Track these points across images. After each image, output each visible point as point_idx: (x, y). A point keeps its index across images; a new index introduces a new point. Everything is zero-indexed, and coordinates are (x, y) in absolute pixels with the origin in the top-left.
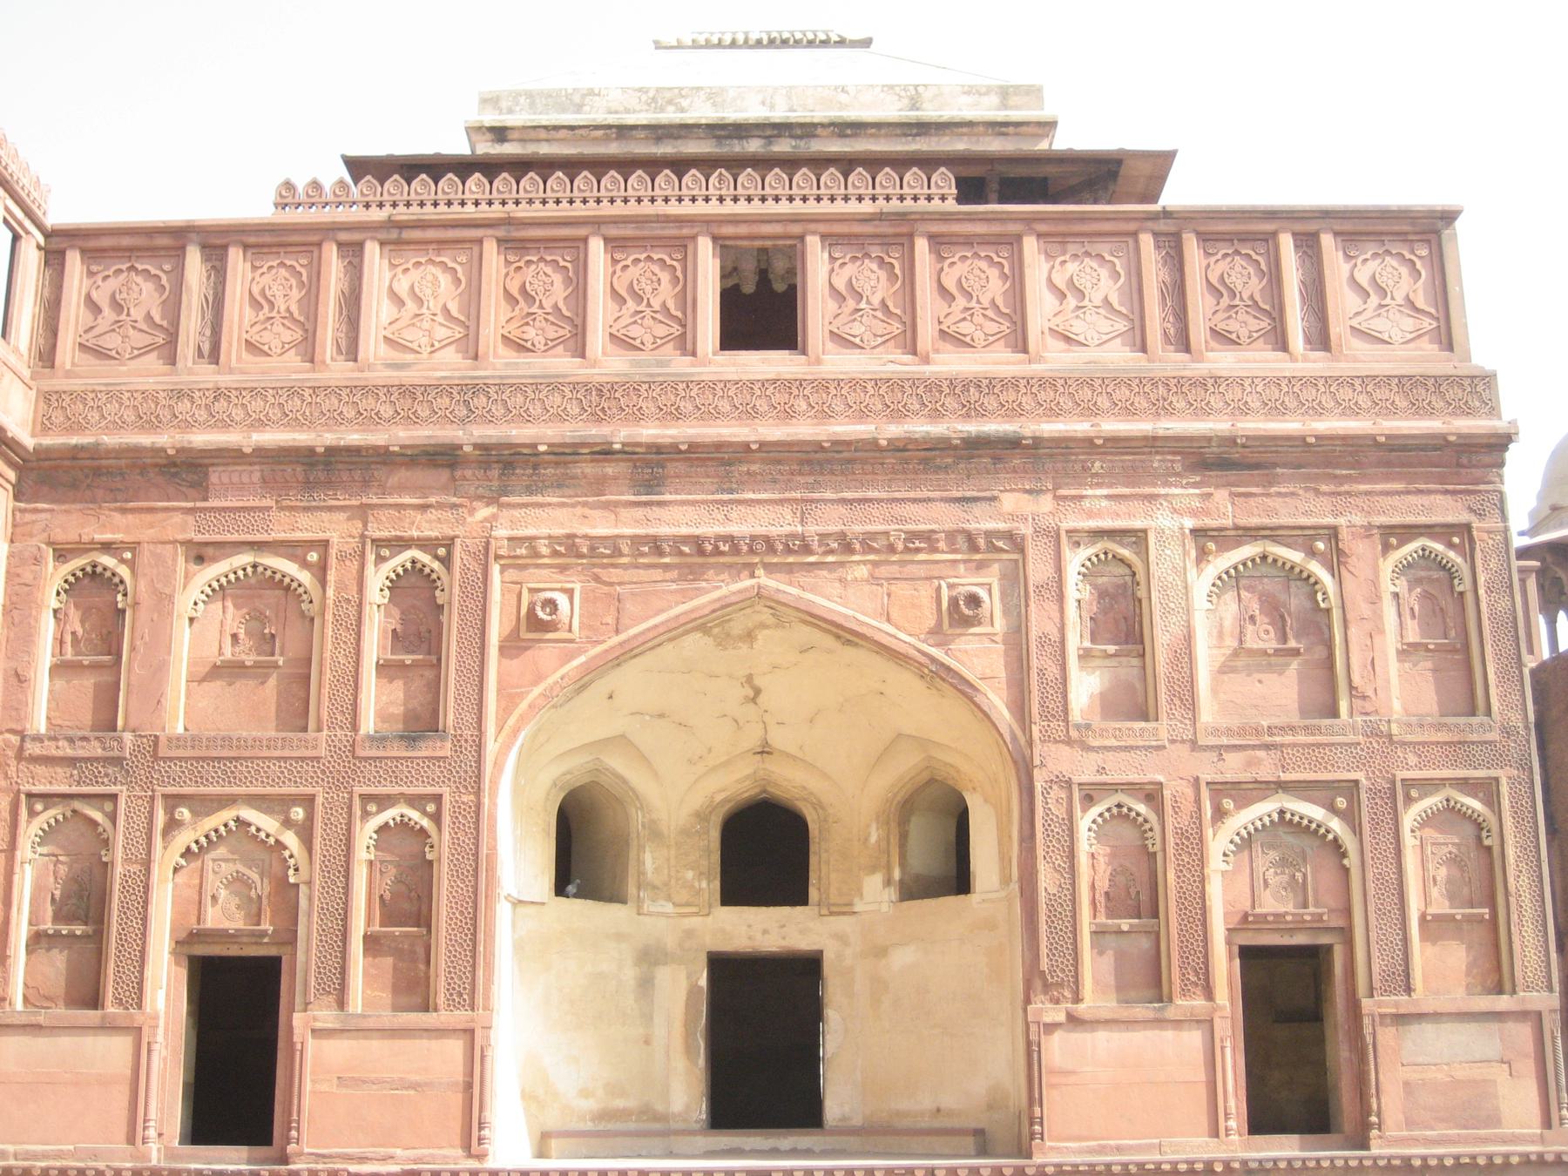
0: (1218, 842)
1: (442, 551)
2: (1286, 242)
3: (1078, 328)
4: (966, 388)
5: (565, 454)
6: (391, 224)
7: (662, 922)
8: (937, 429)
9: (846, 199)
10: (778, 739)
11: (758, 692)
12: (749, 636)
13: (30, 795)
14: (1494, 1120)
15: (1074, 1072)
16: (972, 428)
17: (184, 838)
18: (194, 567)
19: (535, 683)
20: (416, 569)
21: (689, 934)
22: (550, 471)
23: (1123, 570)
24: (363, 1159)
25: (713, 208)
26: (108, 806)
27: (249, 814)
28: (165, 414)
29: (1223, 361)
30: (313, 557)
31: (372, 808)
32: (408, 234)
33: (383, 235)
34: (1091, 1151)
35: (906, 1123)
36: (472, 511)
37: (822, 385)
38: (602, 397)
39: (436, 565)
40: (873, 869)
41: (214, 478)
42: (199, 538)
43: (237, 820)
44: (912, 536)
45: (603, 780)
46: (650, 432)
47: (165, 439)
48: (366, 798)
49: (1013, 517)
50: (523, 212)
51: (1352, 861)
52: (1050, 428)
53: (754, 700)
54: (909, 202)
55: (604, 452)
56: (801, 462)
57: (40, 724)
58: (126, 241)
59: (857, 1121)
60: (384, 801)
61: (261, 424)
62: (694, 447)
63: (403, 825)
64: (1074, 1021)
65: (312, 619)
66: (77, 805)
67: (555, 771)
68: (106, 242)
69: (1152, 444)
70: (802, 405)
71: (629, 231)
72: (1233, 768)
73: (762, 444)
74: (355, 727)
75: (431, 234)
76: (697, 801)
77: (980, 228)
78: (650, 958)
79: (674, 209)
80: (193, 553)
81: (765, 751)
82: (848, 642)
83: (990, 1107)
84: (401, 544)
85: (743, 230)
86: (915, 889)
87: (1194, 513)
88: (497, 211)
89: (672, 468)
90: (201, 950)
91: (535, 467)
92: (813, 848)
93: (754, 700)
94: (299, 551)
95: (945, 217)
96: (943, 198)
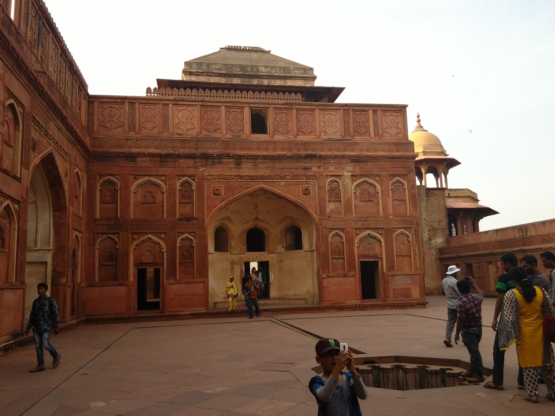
0: (357, 240)
1: (193, 178)
2: (371, 112)
3: (327, 130)
4: (305, 144)
5: (220, 157)
6: (175, 100)
7: (235, 256)
8: (300, 153)
9: (278, 99)
10: (260, 217)
11: (257, 207)
12: (258, 196)
13: (97, 233)
14: (411, 296)
15: (327, 288)
16: (307, 153)
17: (136, 242)
18: (134, 180)
19: (215, 207)
20: (187, 182)
21: (241, 258)
22: (216, 160)
23: (337, 183)
24: (181, 311)
25: (248, 100)
26: (117, 236)
27: (150, 236)
28: (125, 144)
29: (358, 138)
30: (163, 178)
31: (180, 234)
32: (180, 103)
33: (173, 102)
34: (332, 303)
35: (289, 297)
36: (199, 169)
37: (275, 142)
38: (227, 143)
39: (192, 181)
40: (279, 244)
41: (138, 160)
42: (135, 174)
43: (148, 238)
44: (294, 176)
45: (223, 226)
46: (239, 152)
47: (125, 150)
48: (178, 232)
49: (314, 172)
50: (206, 99)
51: (383, 244)
52: (323, 153)
53: (256, 208)
54: (291, 101)
55: (228, 156)
56: (271, 159)
57: (98, 216)
58: (110, 100)
59: (277, 297)
60: (183, 233)
61: (147, 147)
62: (248, 156)
63: (187, 238)
64: (328, 277)
65: (163, 193)
66: (110, 235)
67: (215, 224)
68: (104, 100)
69: (343, 157)
70: (270, 147)
71: (231, 105)
72: (360, 225)
73: (263, 156)
74: (176, 216)
75: (185, 103)
76: (241, 229)
77: (307, 107)
78: (233, 263)
79: (240, 100)
80: (134, 177)
81: (257, 219)
82: (279, 198)
83: (307, 294)
84: (185, 176)
85: (256, 106)
86: (288, 248)
87: (351, 172)
88: (200, 98)
89: (243, 160)
90: (140, 267)
91: (213, 159)
92: (267, 239)
93: (256, 208)
94: (159, 177)
95: (300, 105)
96: (299, 100)
